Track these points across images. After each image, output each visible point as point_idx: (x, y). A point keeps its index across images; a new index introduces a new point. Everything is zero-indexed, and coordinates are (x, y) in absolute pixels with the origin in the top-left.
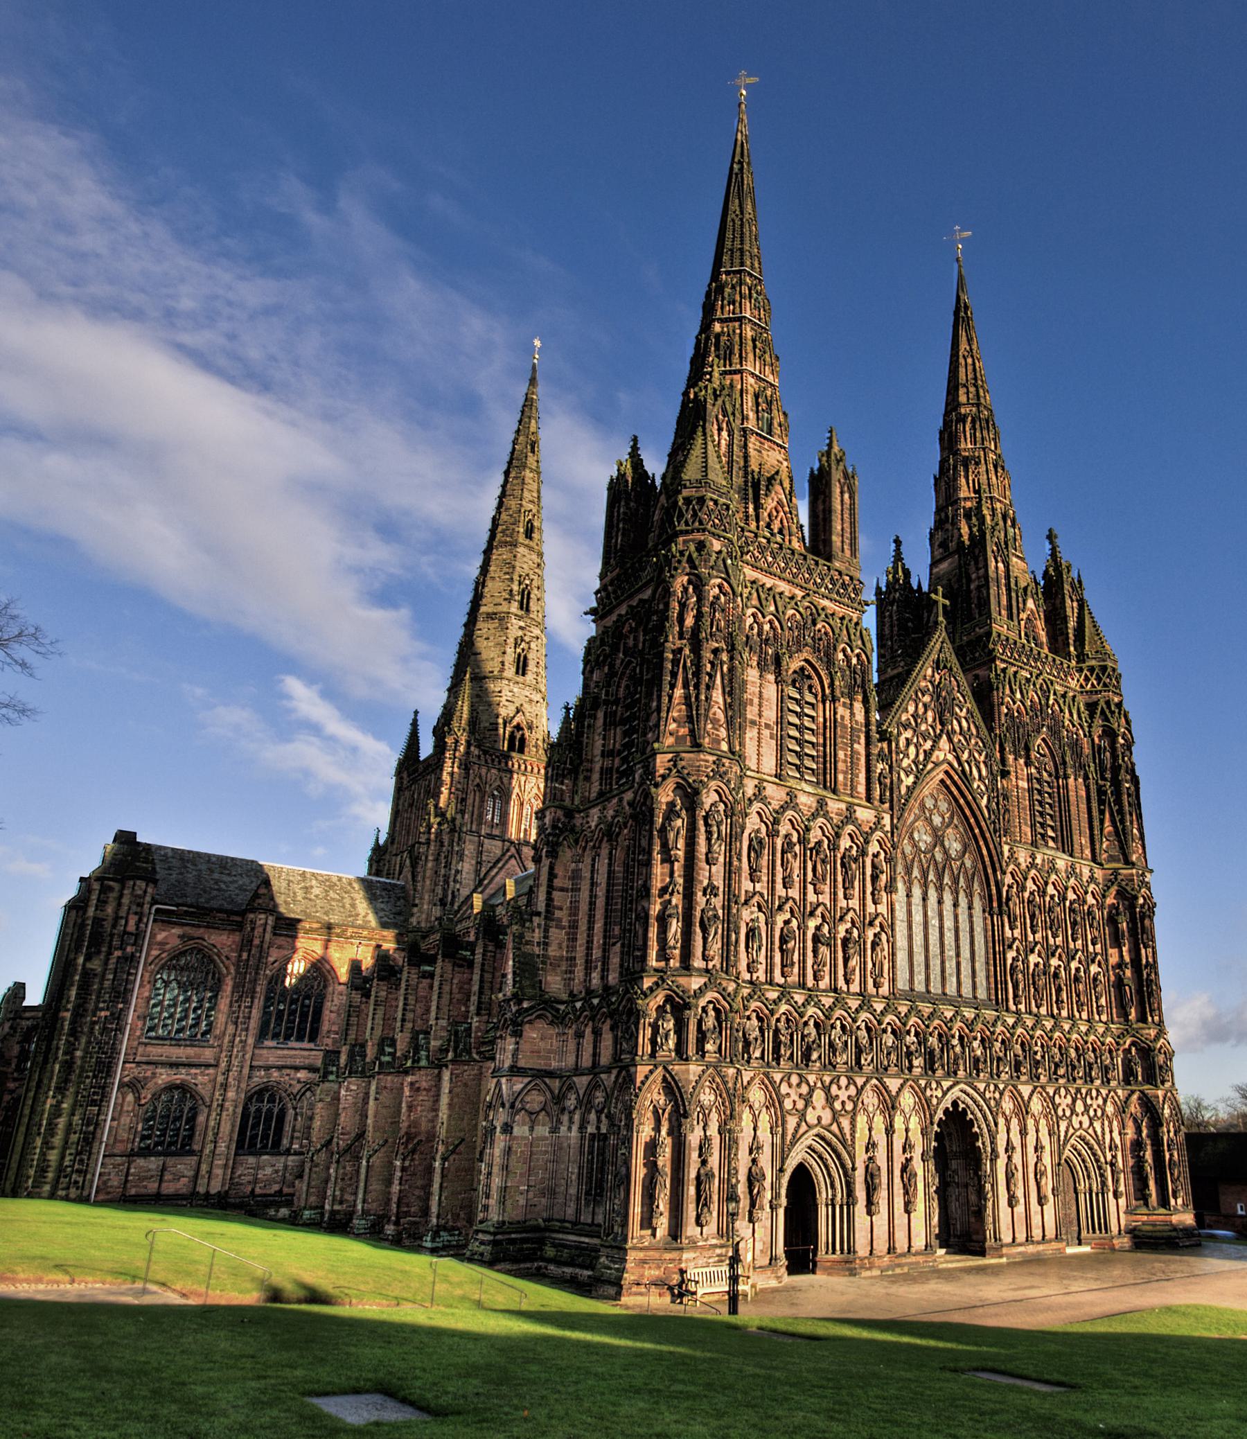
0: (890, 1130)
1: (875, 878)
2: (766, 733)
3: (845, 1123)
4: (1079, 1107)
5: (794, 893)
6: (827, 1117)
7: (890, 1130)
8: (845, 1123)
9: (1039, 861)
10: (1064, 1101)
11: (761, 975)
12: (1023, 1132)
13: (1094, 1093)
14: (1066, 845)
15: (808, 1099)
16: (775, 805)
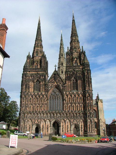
0: (45, 124)
1: (45, 100)
2: (32, 88)
3: (40, 123)
4: (75, 121)
5: (35, 102)
6: (37, 122)
7: (45, 124)
8: (40, 123)
9: (71, 93)
10: (72, 120)
11: (31, 110)
12: (65, 124)
13: (78, 119)
14: (77, 89)
15: (35, 121)
16: (32, 95)
